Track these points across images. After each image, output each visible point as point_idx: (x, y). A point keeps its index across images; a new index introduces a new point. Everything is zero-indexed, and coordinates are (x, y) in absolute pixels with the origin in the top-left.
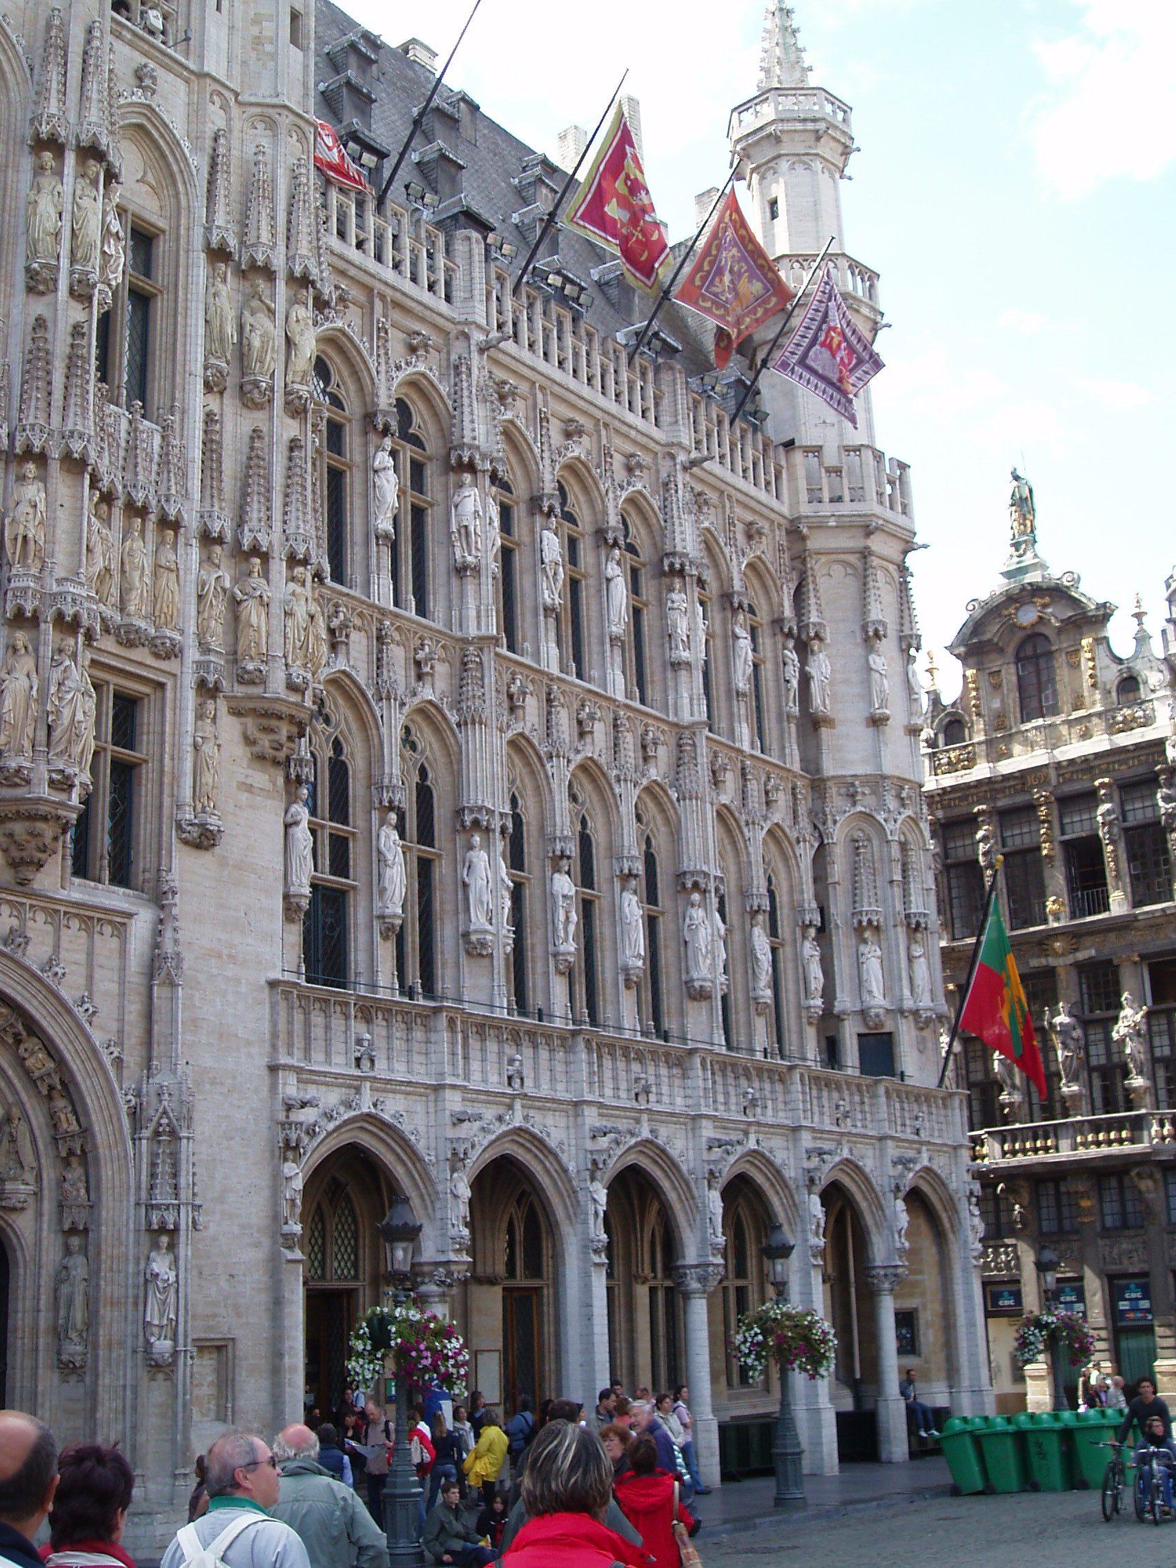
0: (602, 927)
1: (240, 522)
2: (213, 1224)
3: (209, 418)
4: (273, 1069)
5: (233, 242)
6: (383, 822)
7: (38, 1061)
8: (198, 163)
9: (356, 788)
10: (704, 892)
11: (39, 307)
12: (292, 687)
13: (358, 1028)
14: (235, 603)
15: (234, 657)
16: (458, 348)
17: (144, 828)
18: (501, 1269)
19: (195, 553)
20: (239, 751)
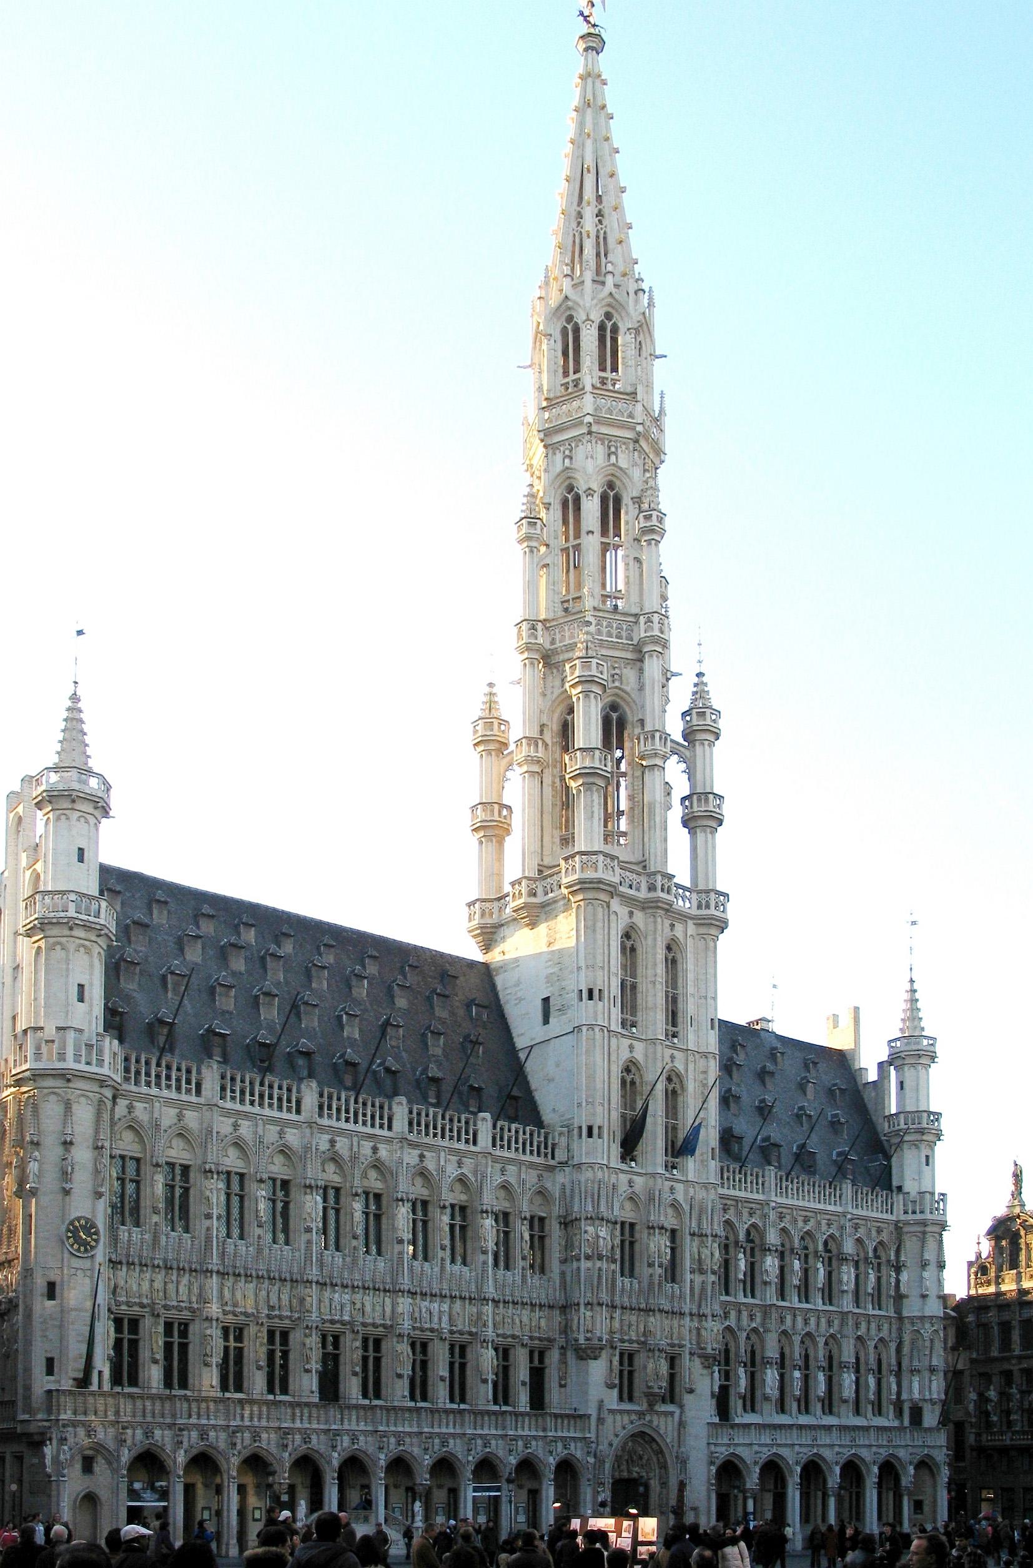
0: (811, 1383)
1: (700, 1306)
2: (694, 1481)
4: (708, 1444)
5: (696, 1231)
6: (740, 1366)
7: (654, 1446)
8: (687, 1208)
9: (732, 1356)
10: (848, 1368)
11: (651, 1271)
12: (713, 1350)
13: (730, 1431)
14: (698, 1329)
15: (698, 1343)
16: (766, 1207)
17: (677, 1390)
18: (772, 1487)
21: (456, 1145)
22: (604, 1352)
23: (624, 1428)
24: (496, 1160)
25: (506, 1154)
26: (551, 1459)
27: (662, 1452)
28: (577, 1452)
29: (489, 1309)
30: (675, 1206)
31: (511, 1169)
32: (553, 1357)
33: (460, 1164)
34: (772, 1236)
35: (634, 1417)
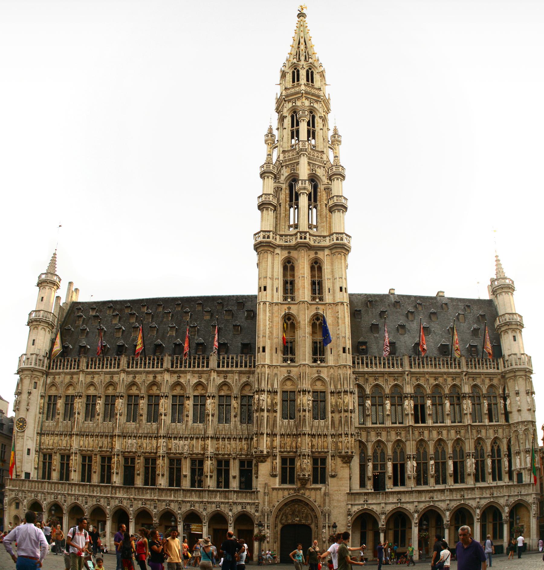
3: (332, 417)
6: (389, 461)
12: (345, 452)
19: (330, 437)
20: (341, 462)
21: (196, 369)
22: (269, 458)
23: (283, 497)
24: (219, 373)
25: (225, 369)
26: (230, 514)
27: (313, 510)
28: (250, 510)
29: (209, 442)
30: (319, 379)
31: (230, 375)
32: (254, 462)
33: (200, 377)
34: (407, 389)
35: (292, 492)
